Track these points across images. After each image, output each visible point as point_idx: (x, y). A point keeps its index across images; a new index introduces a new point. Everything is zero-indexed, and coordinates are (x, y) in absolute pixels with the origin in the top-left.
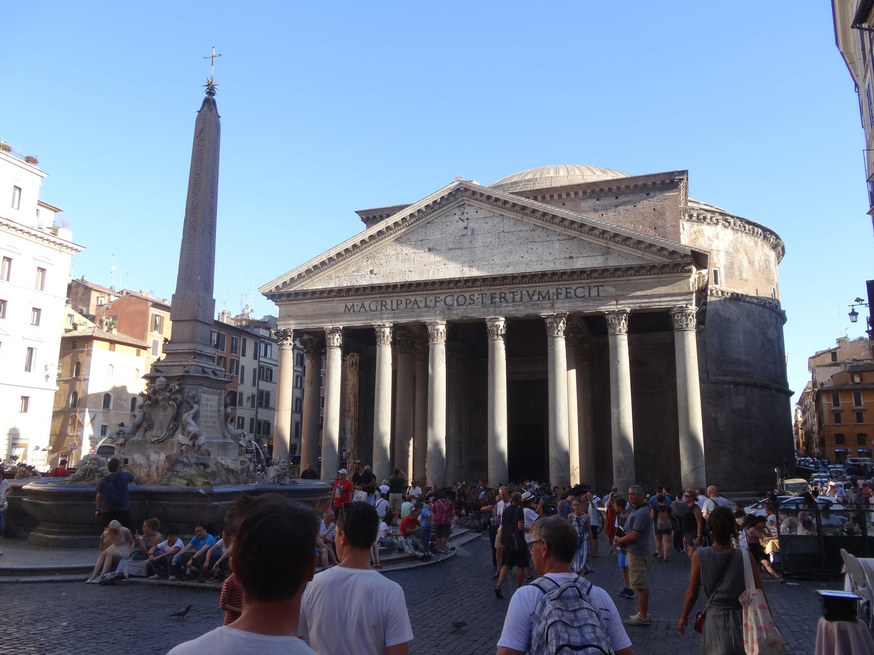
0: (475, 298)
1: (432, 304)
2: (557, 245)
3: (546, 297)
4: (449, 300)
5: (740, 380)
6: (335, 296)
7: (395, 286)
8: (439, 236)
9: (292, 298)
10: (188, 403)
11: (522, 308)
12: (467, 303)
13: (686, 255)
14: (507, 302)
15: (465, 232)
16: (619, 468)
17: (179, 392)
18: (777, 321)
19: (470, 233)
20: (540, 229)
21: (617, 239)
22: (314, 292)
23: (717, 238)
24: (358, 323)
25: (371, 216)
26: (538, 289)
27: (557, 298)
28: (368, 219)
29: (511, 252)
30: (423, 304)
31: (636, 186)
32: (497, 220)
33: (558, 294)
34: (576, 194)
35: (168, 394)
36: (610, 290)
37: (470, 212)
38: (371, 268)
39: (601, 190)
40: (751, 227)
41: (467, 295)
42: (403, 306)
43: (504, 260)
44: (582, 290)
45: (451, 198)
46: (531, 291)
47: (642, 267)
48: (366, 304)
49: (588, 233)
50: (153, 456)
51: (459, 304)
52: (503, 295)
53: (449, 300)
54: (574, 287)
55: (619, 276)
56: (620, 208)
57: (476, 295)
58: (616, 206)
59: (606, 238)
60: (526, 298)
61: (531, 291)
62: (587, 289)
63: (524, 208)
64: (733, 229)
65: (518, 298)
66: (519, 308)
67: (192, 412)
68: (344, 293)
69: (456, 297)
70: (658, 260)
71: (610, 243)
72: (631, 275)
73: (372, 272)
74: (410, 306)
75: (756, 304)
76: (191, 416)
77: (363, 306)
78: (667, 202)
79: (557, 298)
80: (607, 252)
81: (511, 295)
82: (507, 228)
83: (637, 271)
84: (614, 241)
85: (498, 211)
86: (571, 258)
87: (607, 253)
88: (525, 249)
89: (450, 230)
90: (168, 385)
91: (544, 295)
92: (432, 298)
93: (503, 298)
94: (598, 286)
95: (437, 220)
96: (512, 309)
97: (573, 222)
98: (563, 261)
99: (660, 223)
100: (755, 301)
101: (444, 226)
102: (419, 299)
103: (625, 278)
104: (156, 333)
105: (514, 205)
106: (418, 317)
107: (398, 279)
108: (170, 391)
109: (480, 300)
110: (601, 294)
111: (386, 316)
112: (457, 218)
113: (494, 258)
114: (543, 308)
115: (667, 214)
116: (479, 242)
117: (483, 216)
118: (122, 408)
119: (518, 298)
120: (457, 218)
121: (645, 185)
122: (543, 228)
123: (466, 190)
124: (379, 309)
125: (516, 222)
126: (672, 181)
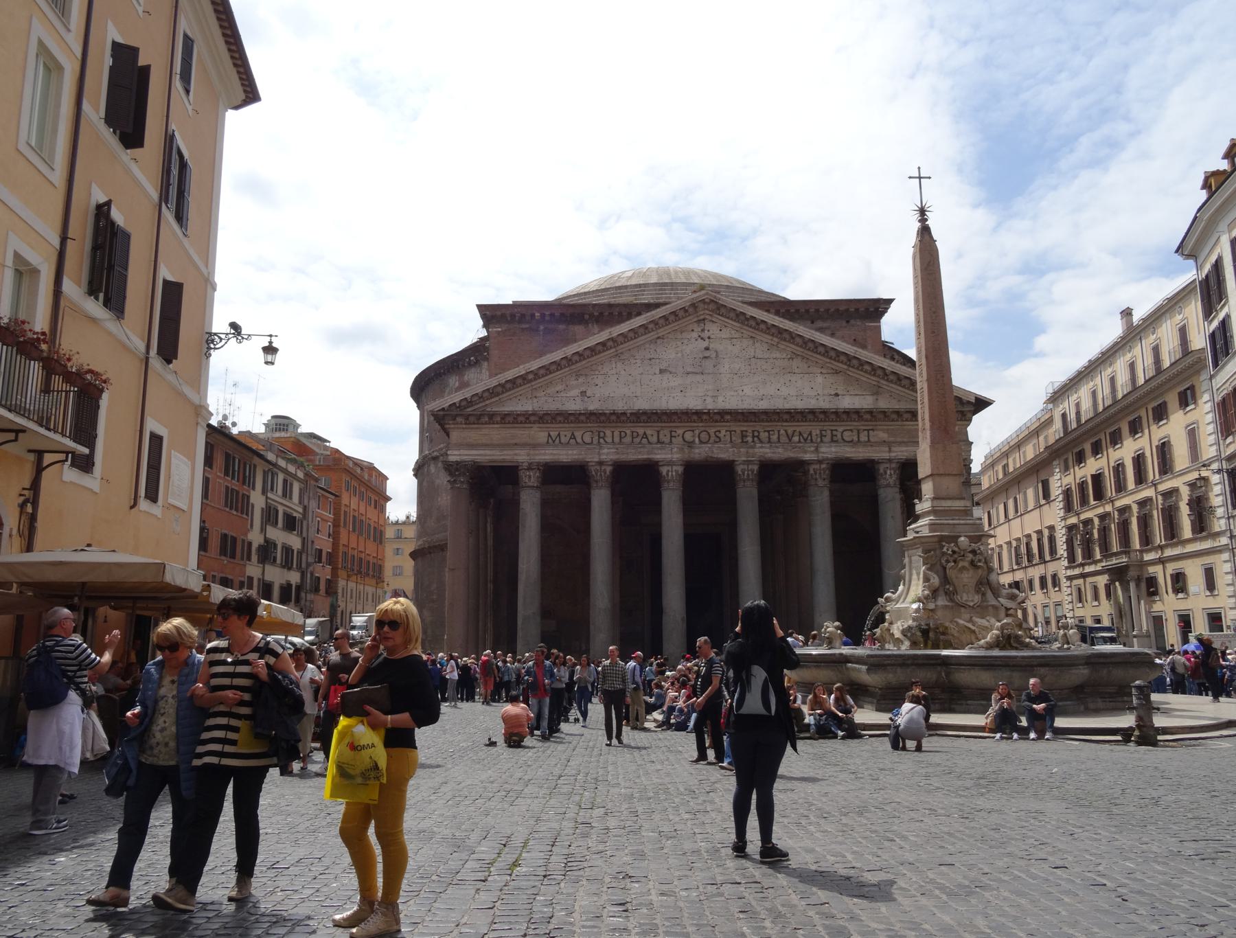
0: (721, 435)
1: (667, 440)
2: (820, 379)
3: (808, 439)
7: (624, 414)
8: (673, 356)
11: (780, 450)
13: (969, 402)
14: (761, 442)
15: (707, 354)
19: (714, 355)
24: (566, 455)
26: (798, 429)
29: (764, 383)
30: (654, 439)
31: (838, 310)
32: (746, 342)
33: (822, 436)
37: (713, 329)
38: (583, 389)
39: (797, 311)
41: (712, 431)
42: (628, 439)
46: (790, 431)
48: (578, 434)
51: (701, 442)
53: (688, 436)
54: (841, 429)
57: (723, 432)
60: (784, 439)
61: (790, 432)
62: (855, 433)
65: (774, 438)
69: (697, 432)
73: (583, 393)
74: (637, 440)
77: (573, 437)
80: (876, 392)
92: (667, 432)
102: (649, 432)
107: (620, 406)
109: (728, 438)
111: (605, 451)
112: (695, 335)
113: (745, 388)
114: (806, 452)
119: (774, 438)
120: (695, 335)
121: (847, 310)
124: (595, 442)
125: (771, 347)
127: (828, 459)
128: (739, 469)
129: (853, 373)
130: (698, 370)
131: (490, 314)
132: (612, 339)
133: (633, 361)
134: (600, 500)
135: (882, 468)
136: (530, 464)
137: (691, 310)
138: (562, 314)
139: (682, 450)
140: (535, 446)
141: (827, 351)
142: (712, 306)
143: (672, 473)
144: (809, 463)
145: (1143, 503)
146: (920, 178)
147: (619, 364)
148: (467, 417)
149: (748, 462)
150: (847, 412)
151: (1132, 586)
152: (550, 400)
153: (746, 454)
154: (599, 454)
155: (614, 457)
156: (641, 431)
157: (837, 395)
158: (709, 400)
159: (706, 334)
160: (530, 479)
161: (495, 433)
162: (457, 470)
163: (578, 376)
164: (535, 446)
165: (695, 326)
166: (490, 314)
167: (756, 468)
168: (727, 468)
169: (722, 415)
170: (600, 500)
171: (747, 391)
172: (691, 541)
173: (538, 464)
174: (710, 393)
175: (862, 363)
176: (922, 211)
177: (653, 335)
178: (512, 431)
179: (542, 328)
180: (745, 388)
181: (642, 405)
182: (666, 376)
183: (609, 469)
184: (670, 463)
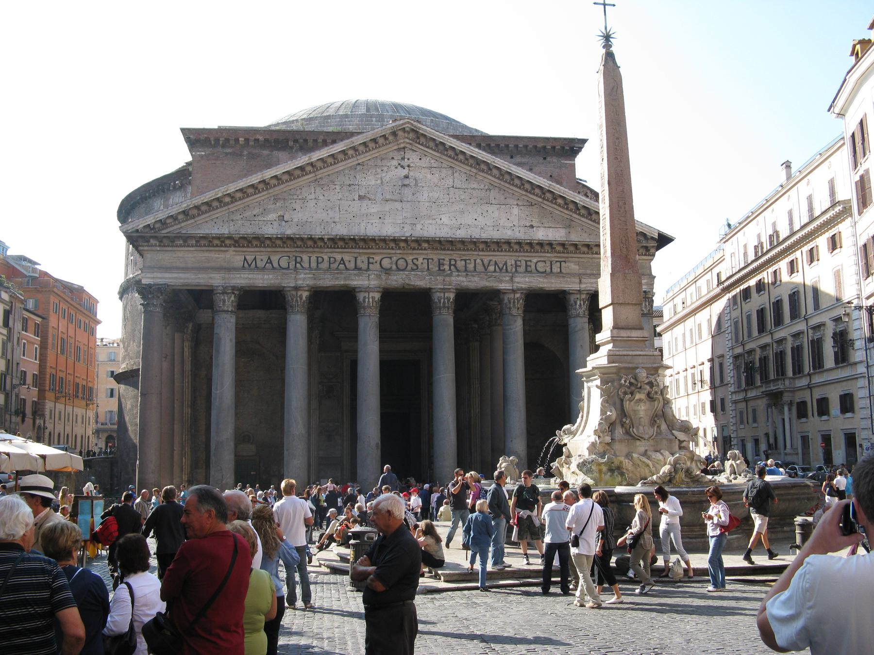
0: (419, 263)
1: (364, 266)
2: (515, 210)
3: (503, 269)
7: (322, 239)
8: (373, 182)
11: (476, 279)
12: (409, 268)
13: (652, 238)
14: (458, 271)
15: (406, 182)
19: (413, 183)
20: (497, 190)
24: (263, 280)
26: (494, 259)
29: (462, 212)
30: (352, 265)
31: (535, 147)
33: (516, 266)
37: (413, 158)
39: (498, 146)
41: (409, 259)
43: (454, 221)
44: (543, 264)
48: (275, 259)
49: (551, 202)
52: (453, 262)
53: (386, 263)
54: (535, 260)
57: (420, 260)
59: (571, 210)
60: (480, 268)
62: (548, 264)
63: (478, 162)
65: (471, 266)
69: (394, 259)
71: (574, 215)
74: (335, 266)
77: (270, 261)
80: (569, 225)
82: (458, 184)
84: (579, 214)
85: (446, 162)
87: (569, 226)
88: (479, 211)
91: (501, 266)
92: (364, 258)
93: (453, 264)
94: (560, 262)
95: (370, 163)
96: (464, 279)
98: (522, 230)
101: (379, 170)
102: (347, 258)
103: (590, 256)
107: (318, 231)
110: (563, 271)
111: (302, 276)
112: (395, 163)
113: (443, 217)
114: (501, 281)
116: (424, 196)
119: (471, 266)
121: (544, 147)
122: (500, 189)
126: (572, 148)
127: (522, 289)
128: (436, 296)
130: (397, 197)
131: (195, 138)
132: (312, 164)
133: (333, 187)
134: (298, 324)
135: (572, 298)
137: (391, 138)
138: (266, 140)
139: (379, 277)
140: (229, 270)
141: (523, 183)
142: (411, 135)
143: (370, 300)
145: (797, 335)
146: (605, 5)
147: (318, 189)
148: (160, 240)
149: (444, 290)
150: (541, 244)
151: (786, 408)
152: (247, 224)
155: (311, 282)
156: (338, 257)
157: (532, 227)
159: (406, 163)
161: (190, 256)
162: (150, 293)
163: (276, 199)
164: (229, 270)
165: (396, 153)
166: (195, 138)
167: (452, 296)
169: (419, 243)
170: (298, 324)
171: (445, 220)
172: (388, 368)
173: (234, 288)
174: (408, 221)
175: (555, 197)
176: (607, 37)
177: (352, 162)
178: (207, 254)
179: (245, 153)
180: (443, 217)
181: (341, 230)
183: (305, 294)
184: (368, 290)
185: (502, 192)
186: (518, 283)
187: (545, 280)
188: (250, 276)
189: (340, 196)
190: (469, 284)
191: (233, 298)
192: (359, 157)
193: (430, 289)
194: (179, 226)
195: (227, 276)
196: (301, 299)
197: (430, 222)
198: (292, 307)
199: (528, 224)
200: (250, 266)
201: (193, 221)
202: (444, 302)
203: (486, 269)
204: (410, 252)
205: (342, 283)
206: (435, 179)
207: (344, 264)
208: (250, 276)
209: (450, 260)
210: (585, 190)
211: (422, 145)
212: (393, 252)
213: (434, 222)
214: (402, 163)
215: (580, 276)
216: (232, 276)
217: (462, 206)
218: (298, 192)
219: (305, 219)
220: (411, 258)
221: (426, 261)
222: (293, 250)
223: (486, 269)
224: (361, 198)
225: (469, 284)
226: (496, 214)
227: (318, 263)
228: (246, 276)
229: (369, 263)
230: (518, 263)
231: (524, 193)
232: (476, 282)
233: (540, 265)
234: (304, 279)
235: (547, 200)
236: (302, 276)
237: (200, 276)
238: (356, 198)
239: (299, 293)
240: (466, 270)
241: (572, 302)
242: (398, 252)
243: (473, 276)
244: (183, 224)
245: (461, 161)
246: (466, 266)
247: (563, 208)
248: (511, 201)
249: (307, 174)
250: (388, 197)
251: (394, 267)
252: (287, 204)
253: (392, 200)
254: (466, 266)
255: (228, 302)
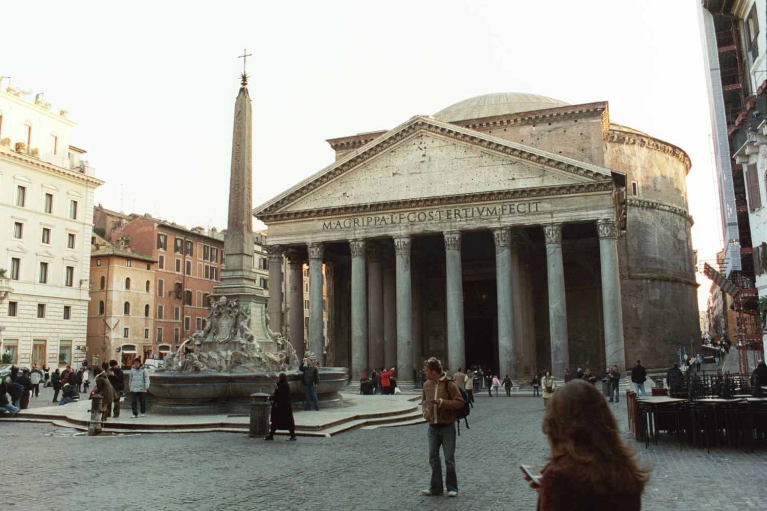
0: (433, 215)
2: (501, 169)
4: (412, 217)
5: (655, 276)
6: (314, 216)
7: (366, 206)
8: (402, 163)
9: (278, 218)
10: (243, 314)
11: (473, 222)
12: (427, 219)
14: (461, 217)
16: (555, 353)
17: (236, 307)
18: (686, 225)
19: (428, 159)
20: (487, 155)
21: (551, 163)
22: (296, 214)
23: (635, 156)
25: (339, 144)
26: (486, 206)
27: (503, 213)
28: (337, 145)
30: (390, 221)
33: (503, 210)
34: (516, 121)
35: (229, 309)
36: (546, 206)
37: (427, 142)
38: (344, 192)
40: (663, 145)
41: (427, 213)
42: (372, 223)
43: (457, 182)
44: (523, 206)
45: (411, 131)
46: (481, 208)
47: (572, 187)
48: (342, 221)
49: (527, 159)
50: (224, 354)
51: (420, 220)
52: (457, 212)
53: (412, 217)
54: (517, 204)
55: (553, 195)
56: (552, 133)
57: (435, 212)
58: (550, 131)
59: (542, 163)
60: (476, 214)
61: (481, 208)
62: (527, 205)
63: (473, 138)
64: (648, 148)
65: (470, 214)
66: (471, 222)
67: (247, 320)
68: (322, 214)
69: (417, 214)
70: (587, 180)
71: (546, 167)
72: (563, 194)
74: (378, 223)
75: (668, 211)
76: (246, 323)
77: (339, 224)
78: (592, 128)
79: (503, 213)
80: (543, 174)
81: (464, 211)
82: (459, 155)
83: (568, 190)
84: (549, 165)
86: (513, 179)
87: (543, 175)
89: (410, 157)
90: (228, 302)
91: (491, 211)
94: (536, 203)
95: (399, 149)
96: (465, 223)
97: (514, 150)
98: (507, 182)
99: (586, 145)
100: (668, 208)
101: (406, 154)
103: (559, 196)
104: (161, 250)
105: (465, 136)
106: (385, 231)
107: (368, 201)
108: (230, 306)
109: (438, 216)
110: (539, 209)
111: (358, 231)
112: (416, 147)
114: (492, 222)
115: (592, 138)
117: (438, 145)
118: (138, 313)
119: (470, 214)
120: (416, 147)
121: (573, 113)
122: (489, 155)
123: (423, 124)
124: (352, 226)
125: (467, 150)
126: (595, 110)
128: (446, 236)
129: (526, 162)
130: (418, 171)
131: (338, 145)
135: (546, 229)
136: (313, 243)
140: (315, 232)
143: (401, 243)
144: (495, 229)
149: (451, 233)
152: (325, 201)
153: (450, 226)
154: (354, 234)
155: (364, 235)
158: (425, 191)
159: (422, 146)
160: (314, 253)
164: (315, 232)
165: (416, 140)
167: (457, 237)
168: (440, 235)
170: (357, 264)
180: (449, 180)
181: (381, 199)
182: (396, 176)
183: (361, 244)
184: (400, 237)
185: (491, 157)
186: (504, 222)
187: (525, 218)
188: (328, 234)
189: (381, 175)
190: (468, 226)
191: (318, 250)
192: (391, 147)
193: (442, 232)
194: (285, 207)
195: (314, 236)
196: (359, 246)
197: (440, 185)
198: (353, 252)
199: (511, 178)
200: (327, 228)
201: (293, 203)
202: (451, 241)
203: (481, 214)
204: (427, 208)
205: (383, 233)
206: (443, 154)
207: (385, 221)
208: (328, 234)
209: (455, 210)
210: (641, 138)
211: (432, 132)
212: (415, 209)
213: (443, 185)
214: (422, 146)
215: (552, 213)
216: (317, 235)
217: (462, 171)
218: (355, 176)
219: (359, 194)
220: (428, 212)
221: (438, 213)
222: (351, 215)
223: (481, 214)
224: (394, 174)
225: (468, 226)
226: (487, 172)
227: (368, 222)
228: (324, 235)
229: (400, 218)
230: (504, 207)
231: (506, 155)
232: (473, 225)
233: (520, 207)
234: (360, 233)
235: (524, 158)
236: (358, 231)
237: (299, 237)
238: (391, 175)
239: (357, 243)
240: (466, 217)
241: (547, 232)
242: (418, 209)
243: (471, 220)
244: (287, 206)
245: (459, 139)
246: (466, 214)
247: (536, 162)
248: (497, 162)
249: (358, 164)
250: (412, 171)
251: (417, 219)
252: (348, 185)
253: (415, 173)
254: (466, 214)
255: (314, 253)
